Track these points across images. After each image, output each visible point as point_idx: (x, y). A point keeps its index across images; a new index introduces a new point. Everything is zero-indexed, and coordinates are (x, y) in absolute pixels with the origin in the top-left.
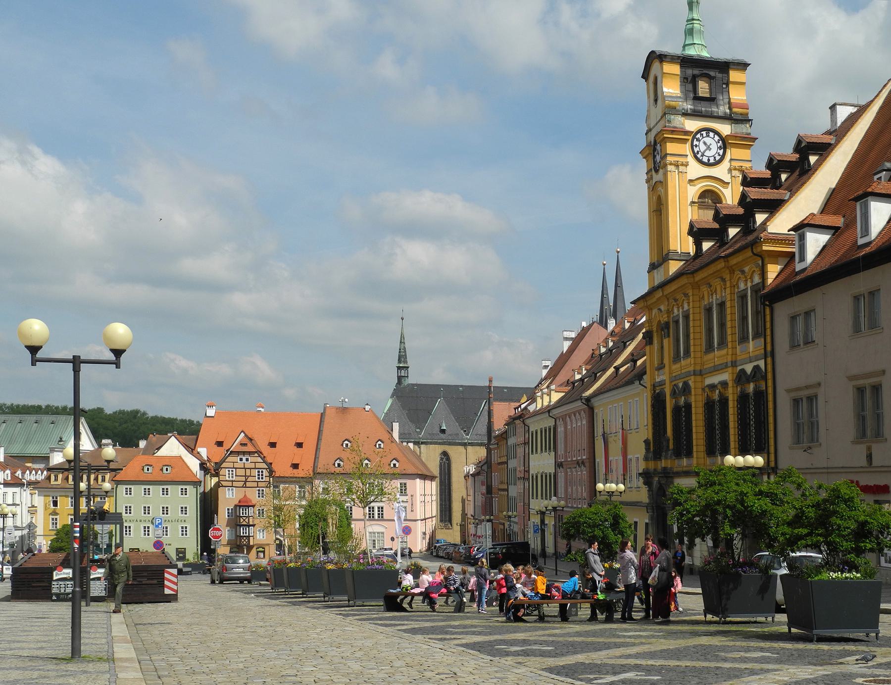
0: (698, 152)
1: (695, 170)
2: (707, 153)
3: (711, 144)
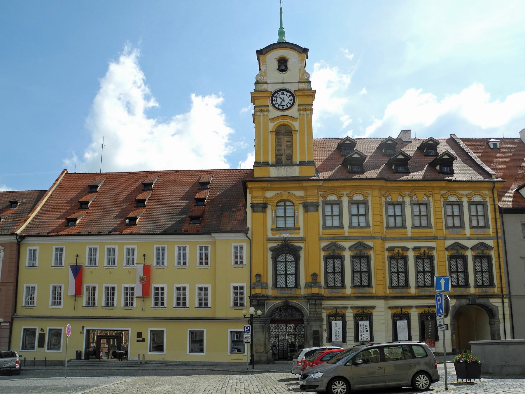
0: (276, 104)
1: (274, 113)
2: (283, 104)
3: (284, 98)
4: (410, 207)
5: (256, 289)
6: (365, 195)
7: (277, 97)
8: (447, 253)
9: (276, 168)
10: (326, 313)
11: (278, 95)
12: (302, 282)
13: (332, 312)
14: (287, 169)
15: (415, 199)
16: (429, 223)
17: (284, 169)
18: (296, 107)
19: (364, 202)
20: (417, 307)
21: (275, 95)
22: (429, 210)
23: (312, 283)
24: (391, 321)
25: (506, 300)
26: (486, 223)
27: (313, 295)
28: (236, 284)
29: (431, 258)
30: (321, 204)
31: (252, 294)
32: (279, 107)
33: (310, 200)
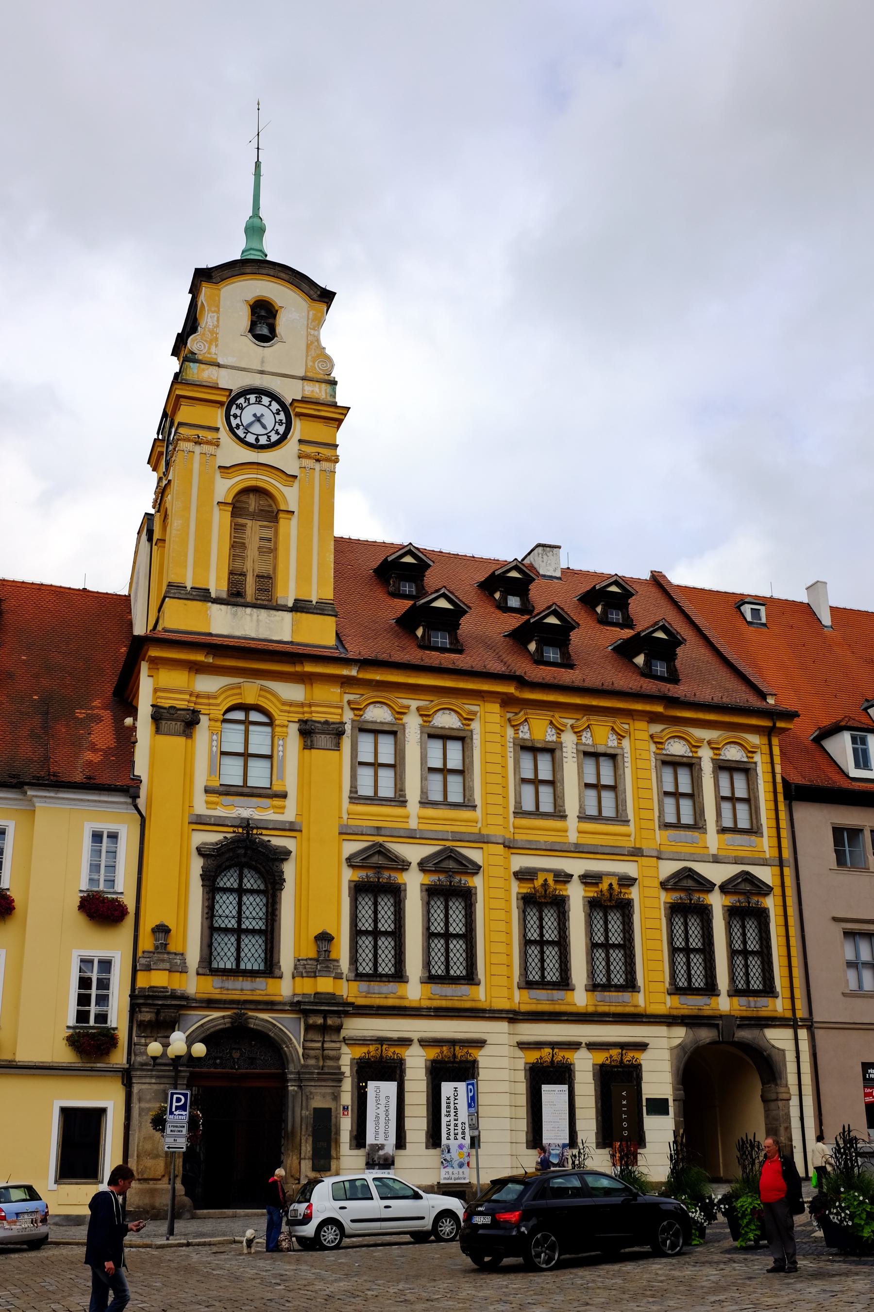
0: (238, 426)
4: (575, 759)
5: (153, 972)
6: (465, 716)
7: (242, 409)
8: (665, 897)
9: (229, 611)
10: (350, 1056)
11: (246, 404)
12: (286, 960)
13: (369, 1053)
14: (260, 618)
15: (587, 739)
16: (620, 807)
17: (251, 615)
18: (292, 446)
19: (461, 734)
21: (238, 402)
22: (620, 772)
23: (317, 960)
24: (524, 1084)
25: (803, 1034)
26: (754, 821)
27: (320, 998)
28: (87, 953)
29: (625, 908)
30: (348, 727)
31: (139, 988)
32: (245, 437)
33: (319, 715)
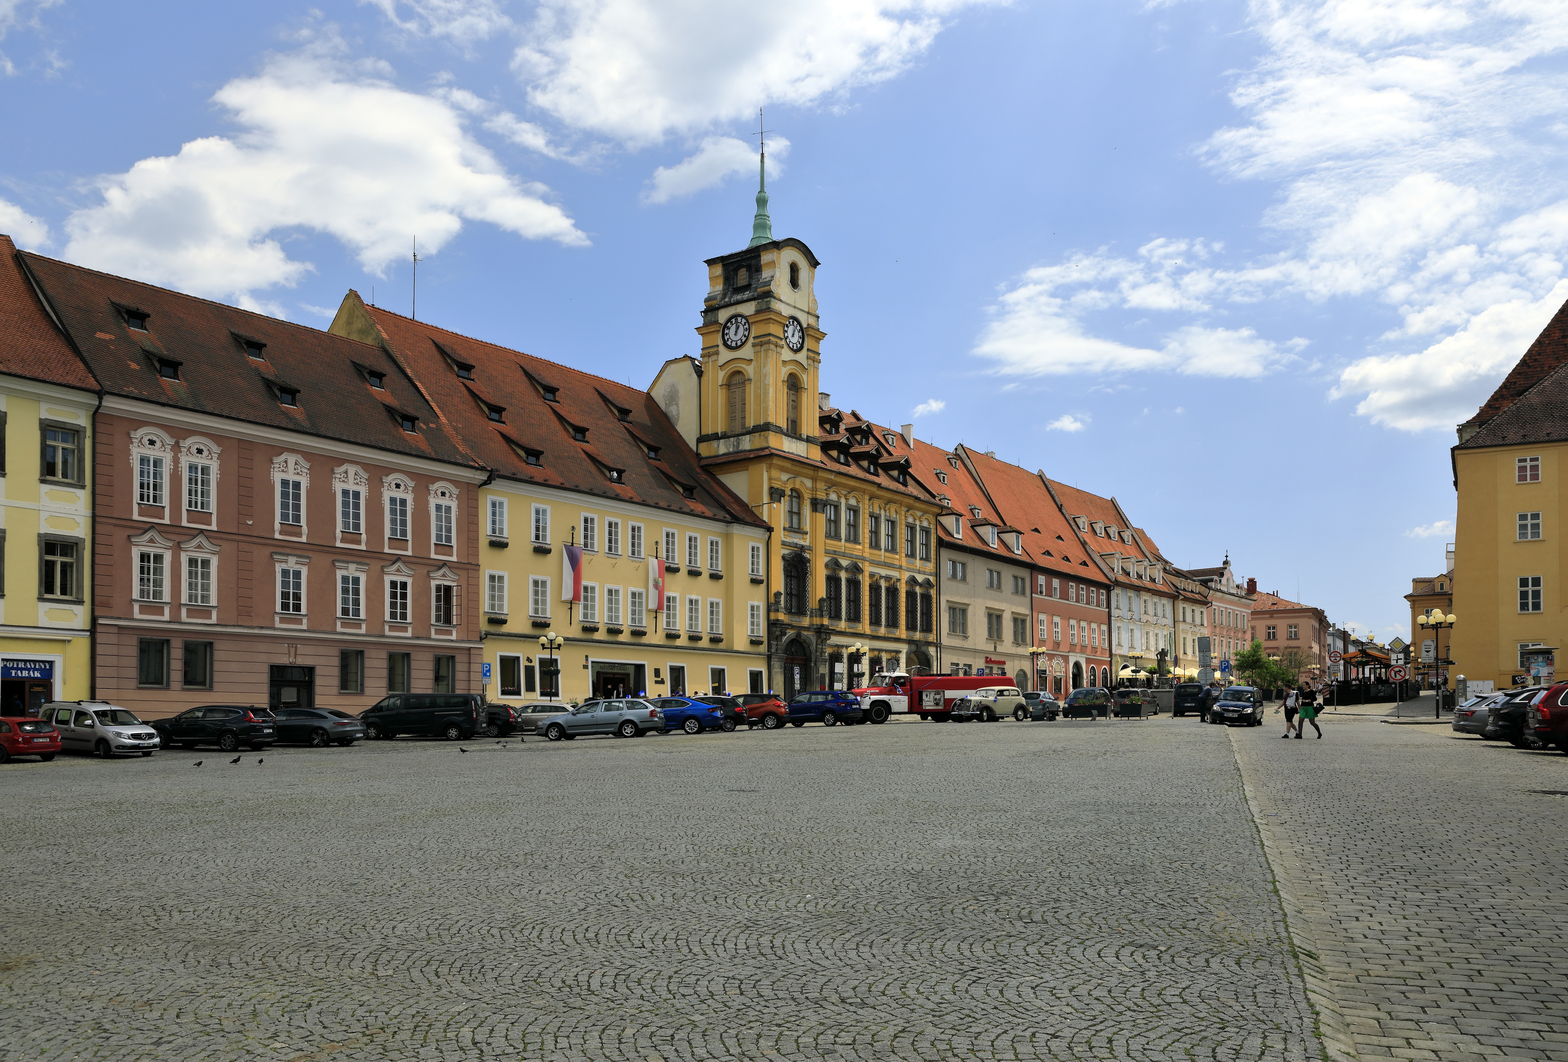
1: (786, 355)
20: (886, 651)
